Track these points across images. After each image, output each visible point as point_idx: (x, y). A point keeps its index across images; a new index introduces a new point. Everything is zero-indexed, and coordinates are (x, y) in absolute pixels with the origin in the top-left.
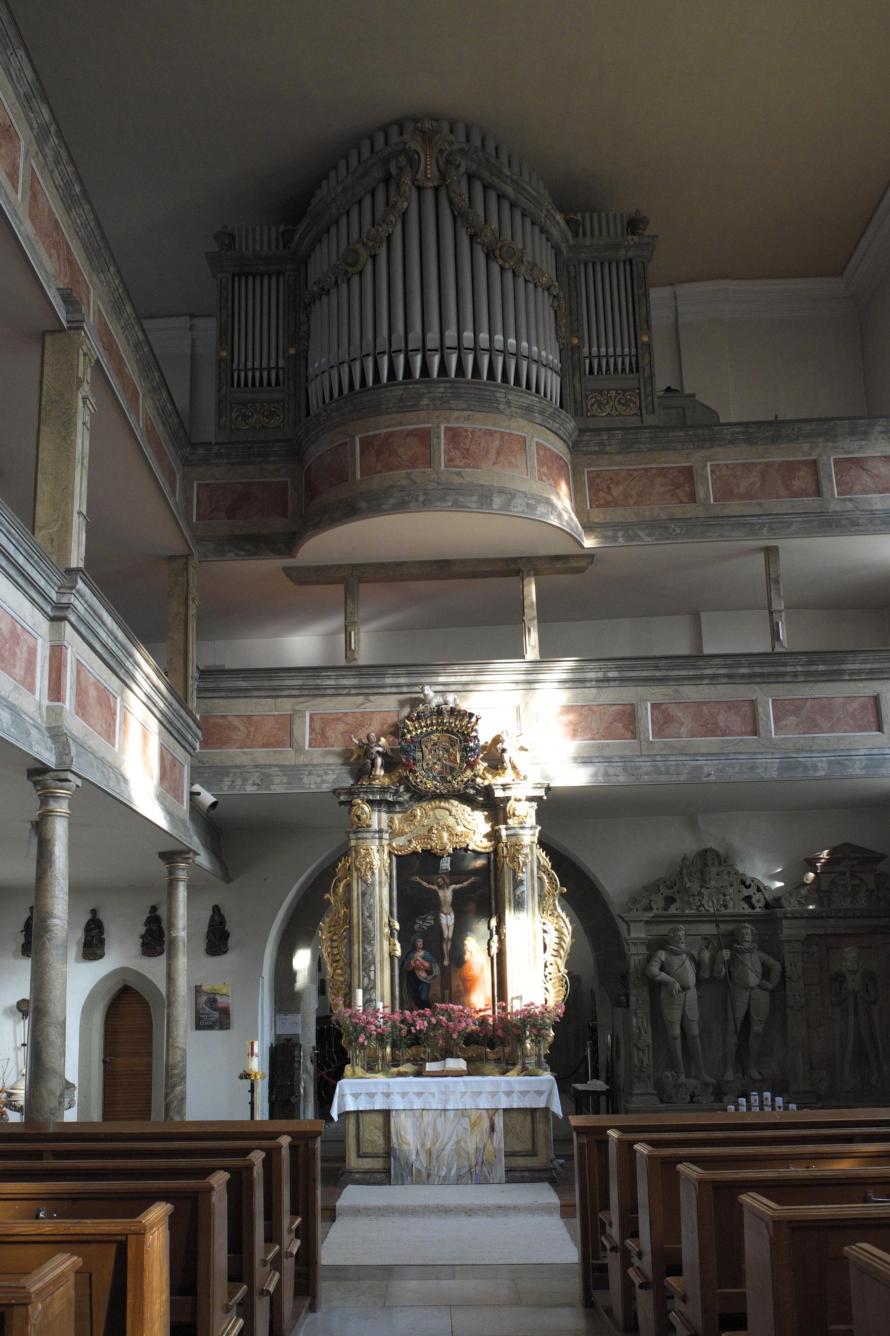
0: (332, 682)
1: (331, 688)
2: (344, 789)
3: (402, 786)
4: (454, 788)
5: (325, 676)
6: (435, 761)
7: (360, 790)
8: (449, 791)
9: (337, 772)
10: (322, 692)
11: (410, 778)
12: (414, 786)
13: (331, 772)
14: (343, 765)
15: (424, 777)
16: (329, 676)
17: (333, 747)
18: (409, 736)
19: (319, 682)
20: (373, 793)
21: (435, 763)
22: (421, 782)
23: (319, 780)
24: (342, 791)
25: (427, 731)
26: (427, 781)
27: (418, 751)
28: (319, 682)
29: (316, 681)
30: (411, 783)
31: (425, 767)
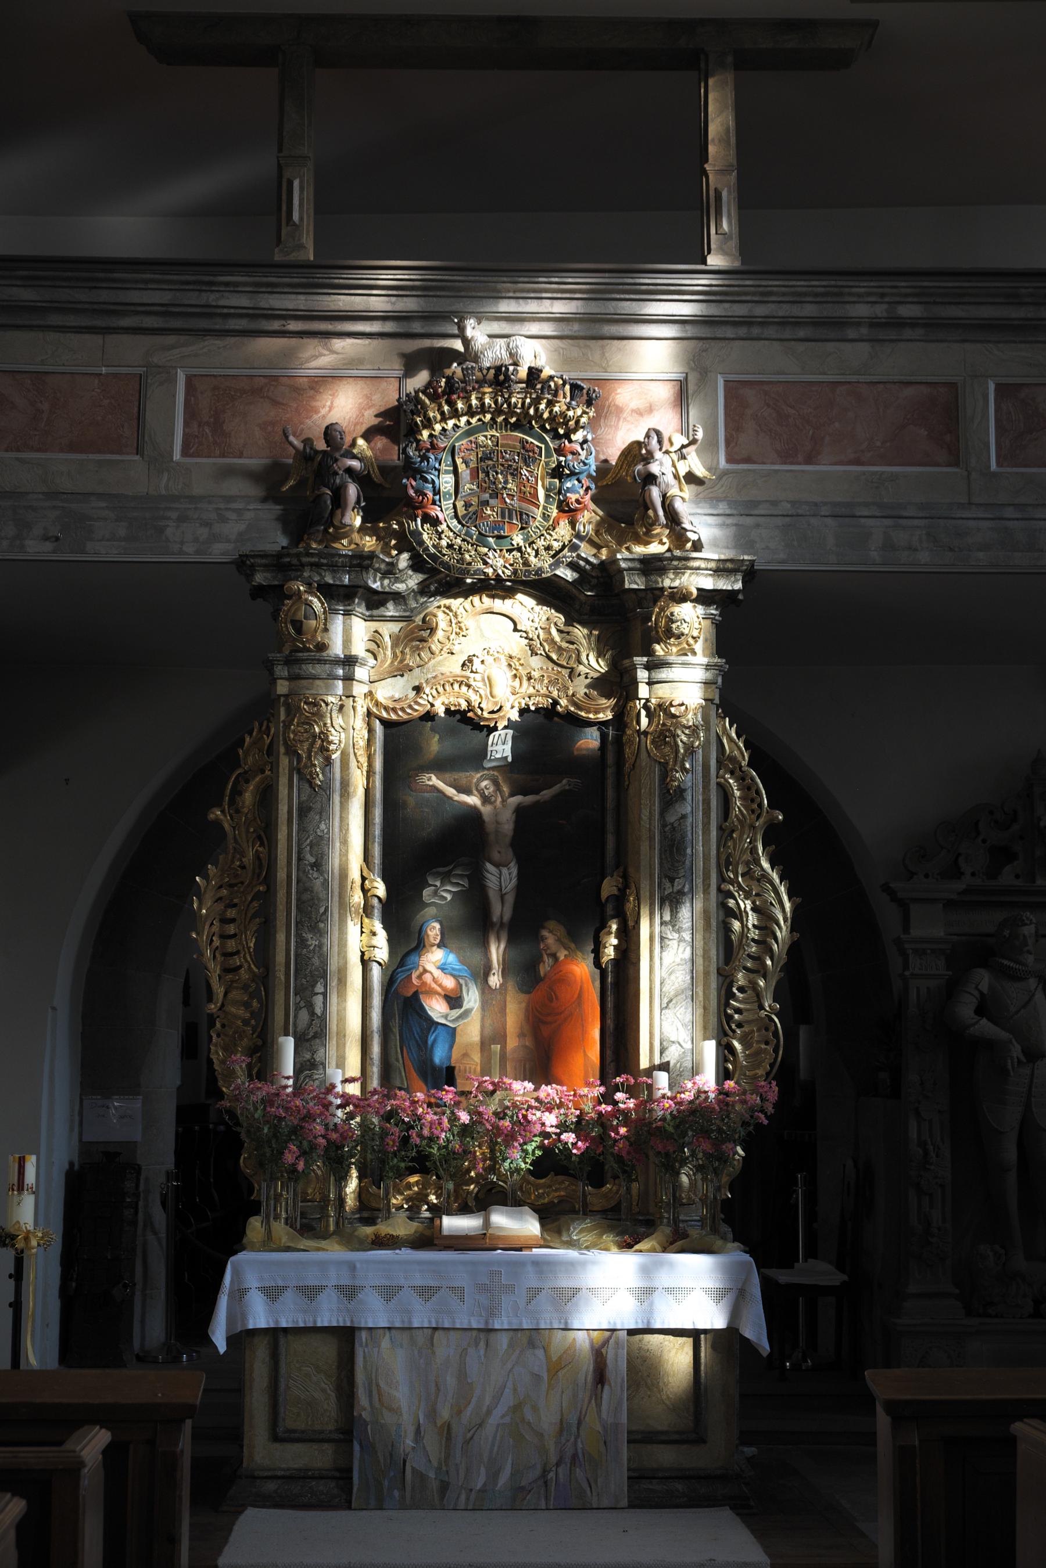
0: (244, 301)
1: (241, 316)
2: (264, 555)
3: (405, 556)
4: (526, 563)
5: (227, 284)
6: (486, 496)
7: (305, 560)
8: (515, 572)
9: (249, 515)
10: (218, 324)
11: (425, 536)
12: (433, 557)
13: (233, 516)
14: (265, 500)
15: (457, 535)
16: (236, 284)
17: (241, 456)
18: (425, 434)
19: (212, 298)
20: (334, 568)
21: (486, 503)
22: (450, 546)
23: (203, 532)
24: (259, 561)
25: (469, 423)
26: (464, 545)
27: (447, 472)
28: (212, 298)
29: (204, 295)
30: (427, 549)
31: (461, 511)
